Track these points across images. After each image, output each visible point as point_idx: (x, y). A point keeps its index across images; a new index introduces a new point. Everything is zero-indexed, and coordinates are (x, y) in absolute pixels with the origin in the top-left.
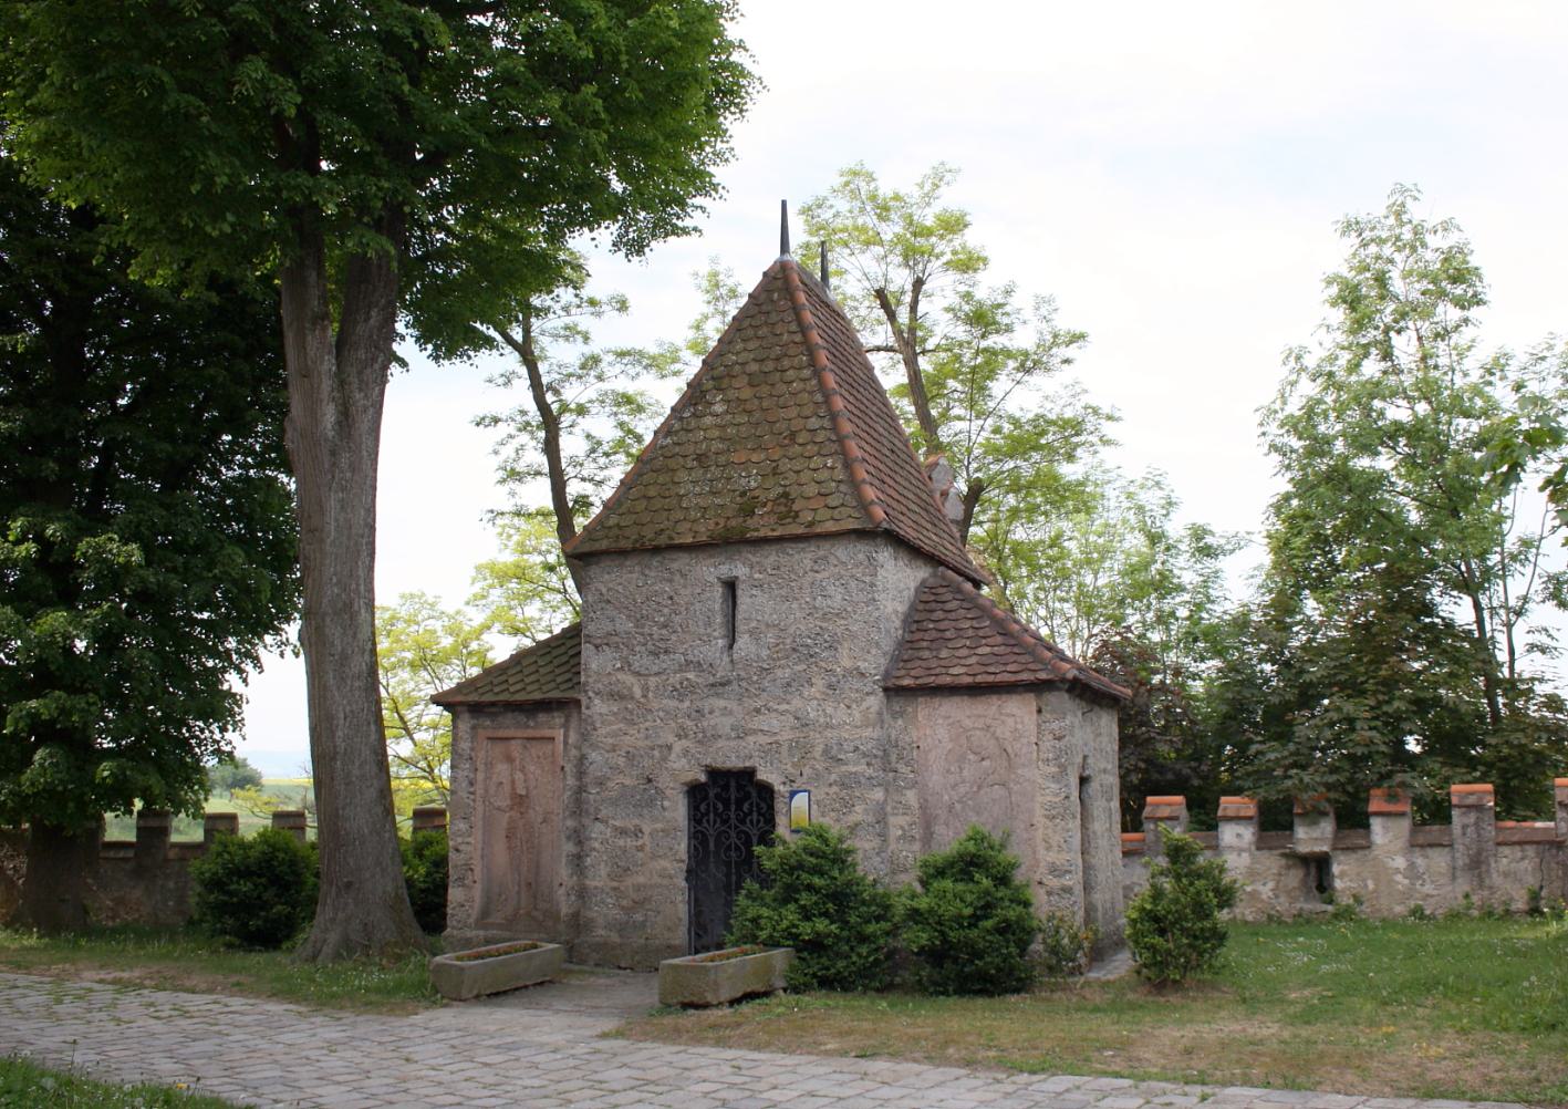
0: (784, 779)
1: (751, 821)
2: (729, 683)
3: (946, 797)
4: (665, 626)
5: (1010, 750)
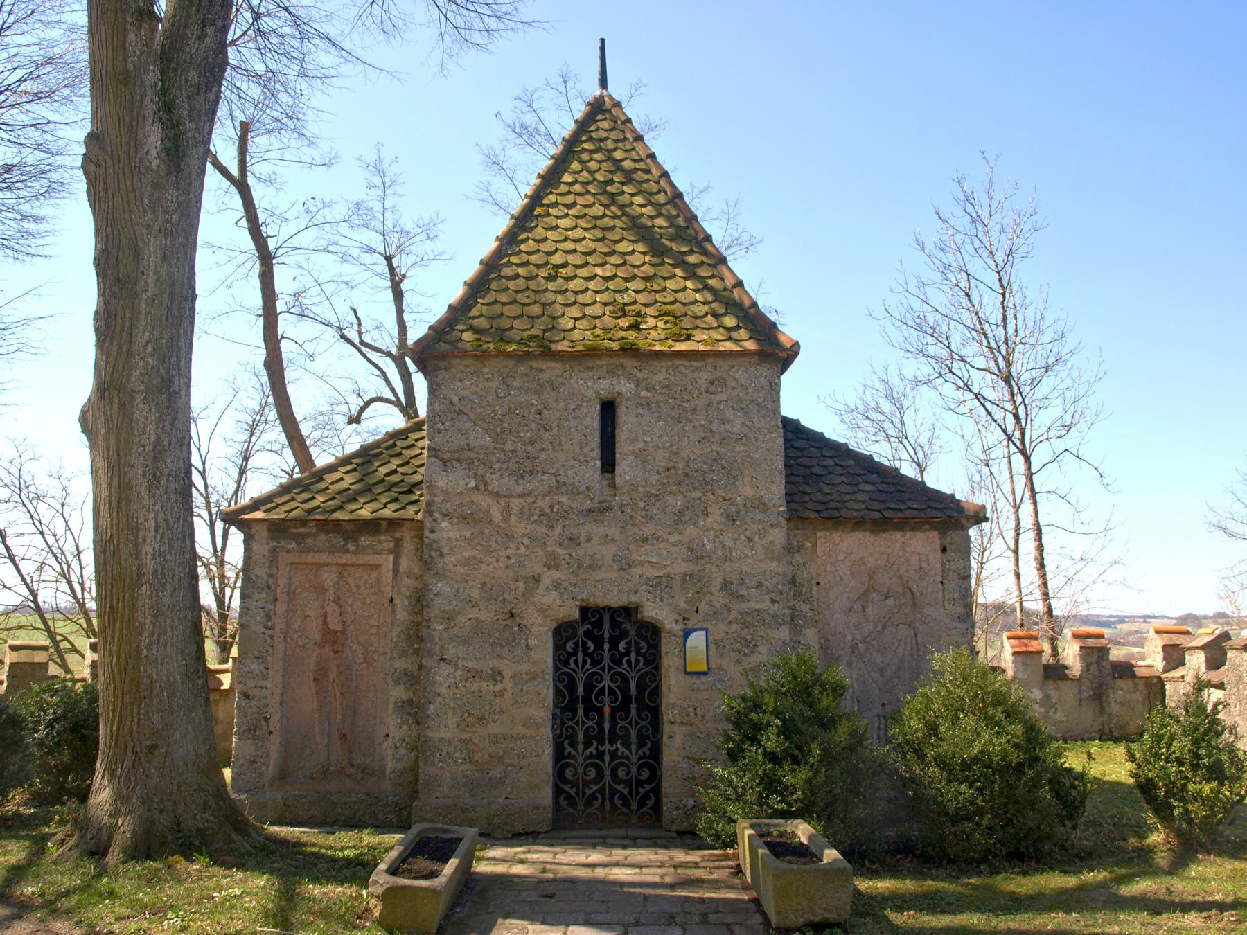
0: (676, 617)
1: (629, 662)
2: (609, 509)
3: (849, 638)
4: (532, 443)
5: (915, 590)
